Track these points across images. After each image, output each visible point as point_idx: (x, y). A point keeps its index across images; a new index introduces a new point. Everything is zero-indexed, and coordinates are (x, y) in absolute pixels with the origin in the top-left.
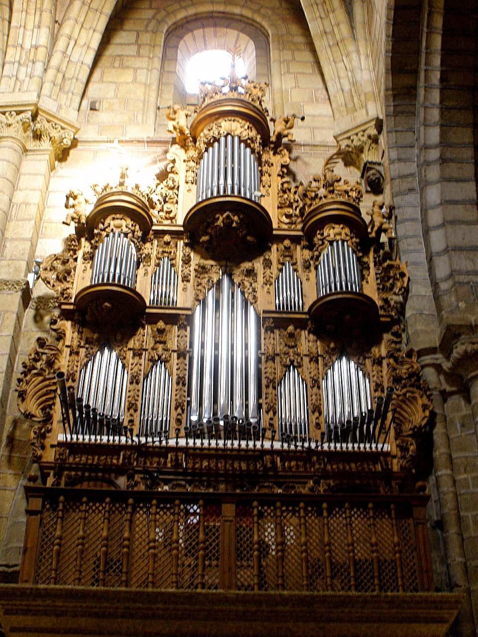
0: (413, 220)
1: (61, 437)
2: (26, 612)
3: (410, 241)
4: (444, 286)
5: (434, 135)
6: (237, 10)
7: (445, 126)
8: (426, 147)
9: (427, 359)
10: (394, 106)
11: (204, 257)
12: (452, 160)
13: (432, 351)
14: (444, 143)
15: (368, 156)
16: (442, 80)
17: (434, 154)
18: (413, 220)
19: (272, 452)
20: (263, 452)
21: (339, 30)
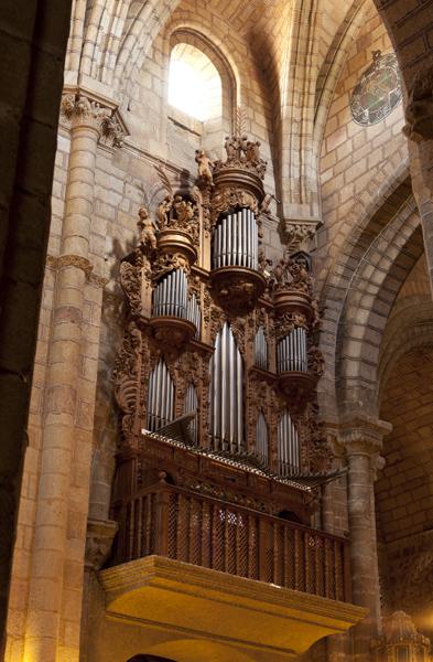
0: (335, 321)
1: (144, 432)
2: (167, 577)
3: (330, 336)
4: (350, 383)
5: (380, 278)
6: (217, 42)
7: (390, 275)
8: (370, 282)
9: (330, 430)
10: (359, 240)
11: (215, 303)
12: (382, 300)
13: (334, 426)
14: (383, 287)
15: (304, 247)
16: (404, 247)
17: (374, 290)
18: (335, 321)
19: (254, 475)
20: (248, 474)
21: (307, 126)
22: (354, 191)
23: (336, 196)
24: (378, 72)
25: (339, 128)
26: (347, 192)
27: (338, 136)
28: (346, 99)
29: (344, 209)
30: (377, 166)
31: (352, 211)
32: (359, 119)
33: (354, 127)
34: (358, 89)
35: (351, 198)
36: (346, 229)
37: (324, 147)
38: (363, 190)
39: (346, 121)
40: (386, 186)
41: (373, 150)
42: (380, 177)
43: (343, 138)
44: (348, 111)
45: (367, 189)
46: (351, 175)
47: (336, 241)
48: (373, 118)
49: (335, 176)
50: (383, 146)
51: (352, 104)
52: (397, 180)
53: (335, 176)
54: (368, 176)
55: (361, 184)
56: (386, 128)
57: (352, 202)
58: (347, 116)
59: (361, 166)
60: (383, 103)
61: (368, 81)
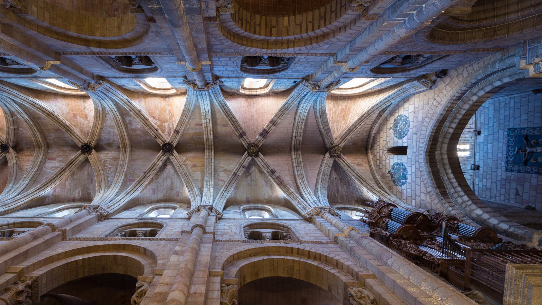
22: (424, 193)
23: (422, 201)
24: (394, 173)
25: (401, 193)
26: (423, 197)
27: (403, 194)
28: (395, 187)
29: (428, 200)
30: (421, 181)
31: (431, 197)
32: (403, 184)
33: (404, 187)
34: (394, 182)
35: (426, 196)
36: (436, 201)
37: (404, 200)
38: (426, 189)
39: (401, 189)
40: (429, 177)
41: (415, 182)
42: (425, 182)
43: (405, 192)
44: (399, 187)
45: (426, 188)
46: (418, 193)
47: (438, 207)
48: (405, 179)
49: (415, 200)
50: (416, 177)
51: (397, 185)
52: (429, 172)
53: (415, 200)
54: (423, 186)
55: (423, 189)
56: (411, 175)
57: (428, 196)
58: (399, 188)
59: (418, 187)
60: (403, 174)
61: (394, 177)
